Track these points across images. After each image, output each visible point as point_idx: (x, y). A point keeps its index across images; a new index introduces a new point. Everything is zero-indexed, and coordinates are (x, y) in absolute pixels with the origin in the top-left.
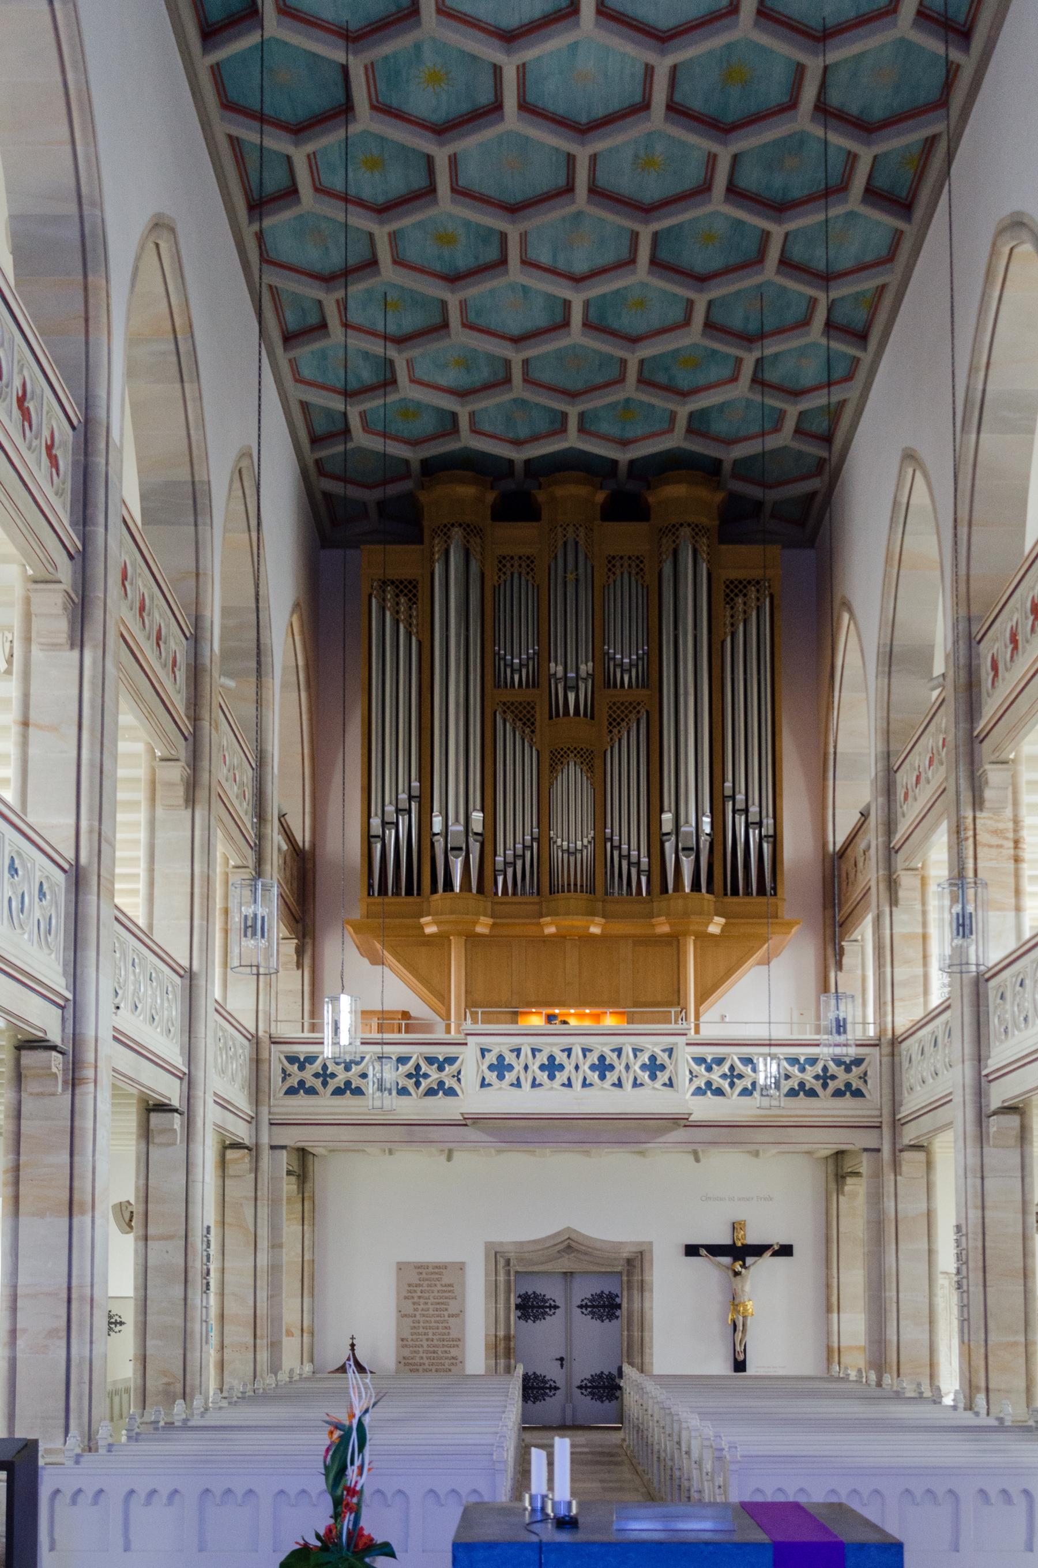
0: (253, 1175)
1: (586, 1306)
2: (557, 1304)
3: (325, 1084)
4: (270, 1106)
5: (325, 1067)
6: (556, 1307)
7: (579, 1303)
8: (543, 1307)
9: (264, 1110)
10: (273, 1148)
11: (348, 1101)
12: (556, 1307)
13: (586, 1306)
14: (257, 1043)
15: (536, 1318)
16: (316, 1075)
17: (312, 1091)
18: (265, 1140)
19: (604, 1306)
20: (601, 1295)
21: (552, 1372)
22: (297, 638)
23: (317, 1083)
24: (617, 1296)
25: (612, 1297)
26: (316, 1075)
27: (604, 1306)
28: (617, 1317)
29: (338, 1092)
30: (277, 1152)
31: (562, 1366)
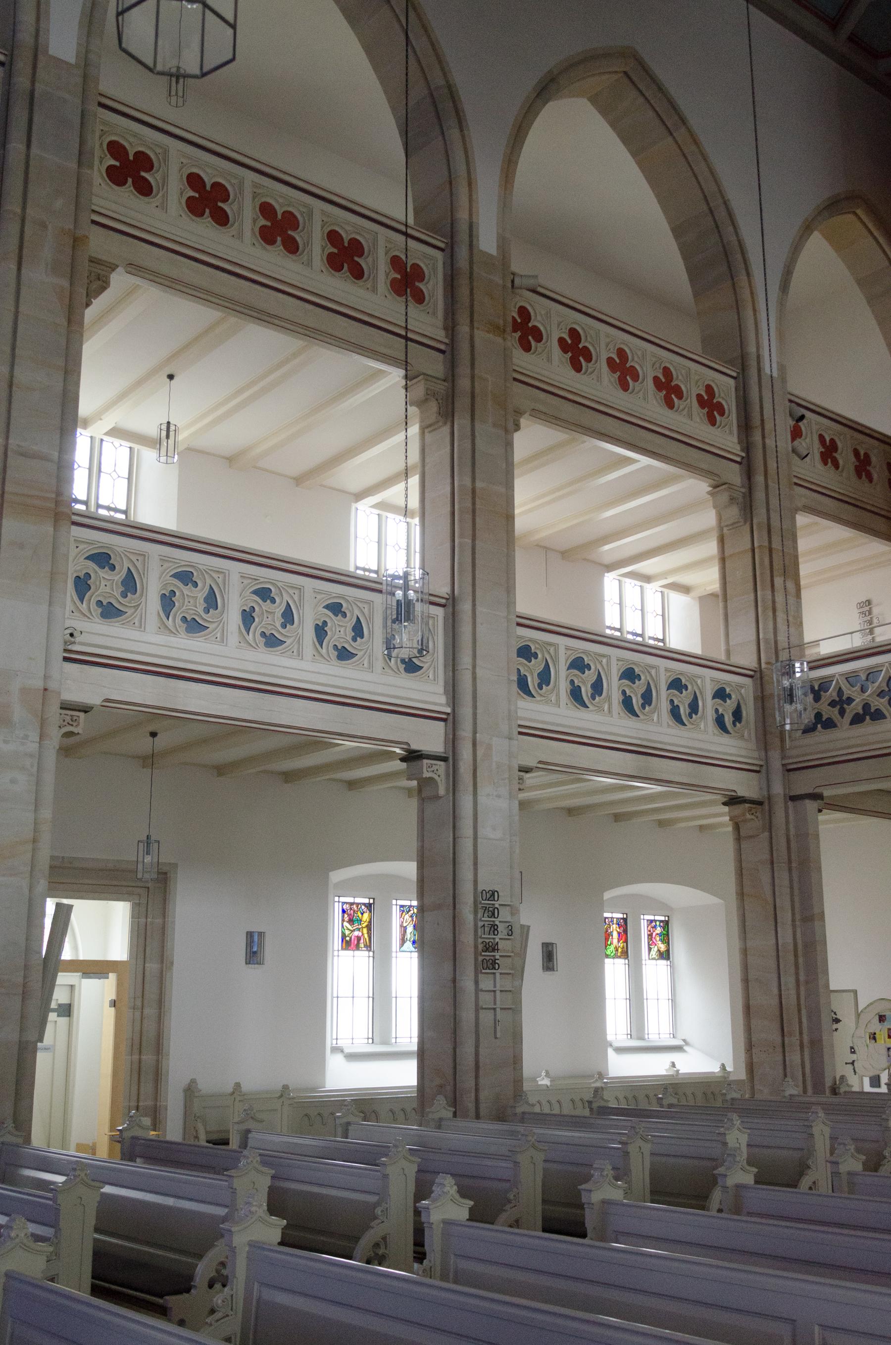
0: (767, 834)
3: (842, 712)
4: (783, 749)
5: (840, 692)
9: (775, 756)
10: (793, 798)
11: (869, 731)
14: (761, 678)
16: (833, 704)
17: (829, 724)
18: (778, 789)
22: (876, 233)
23: (834, 713)
26: (833, 704)
29: (857, 720)
30: (798, 803)
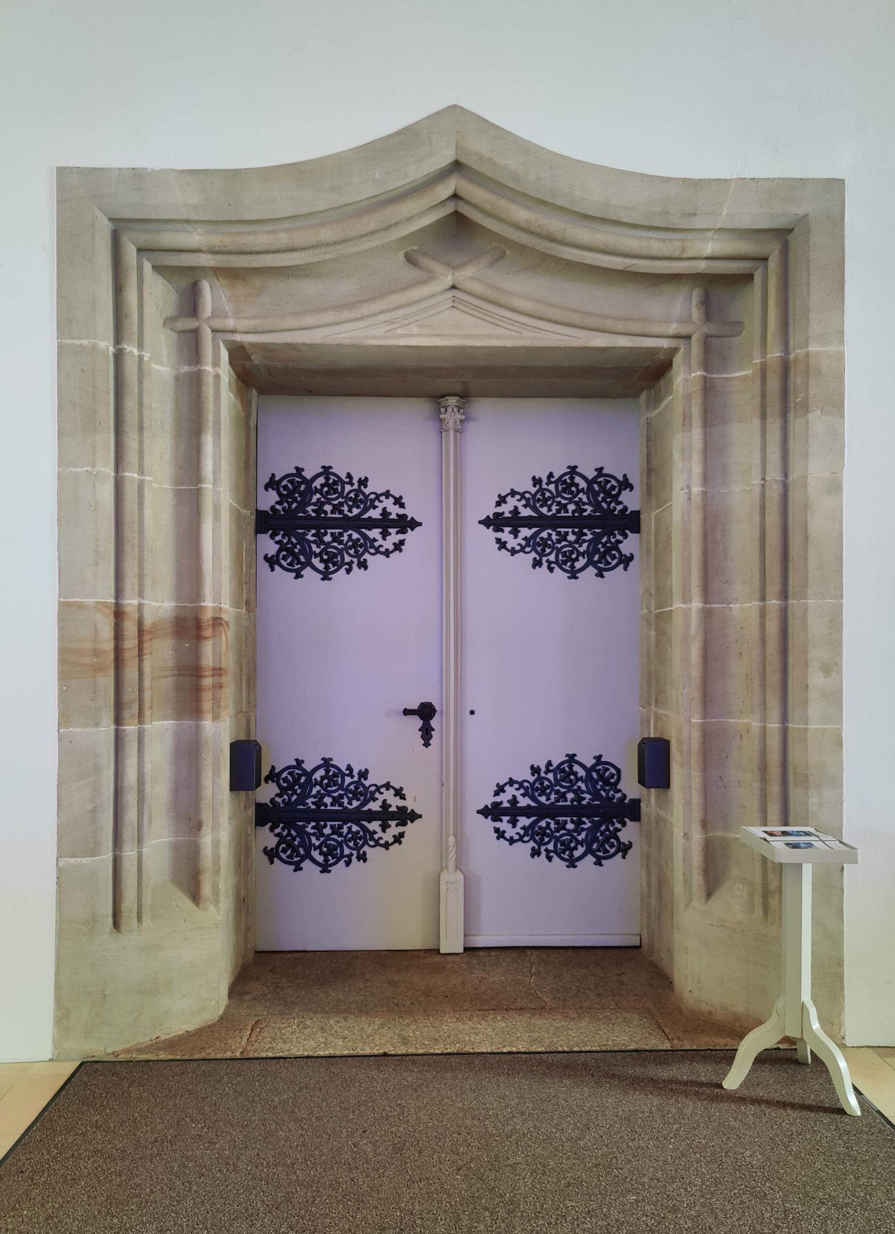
1: (515, 522)
2: (410, 512)
6: (406, 524)
7: (490, 510)
8: (360, 523)
12: (406, 524)
13: (515, 522)
15: (332, 564)
19: (578, 522)
20: (567, 482)
21: (379, 751)
24: (626, 484)
25: (606, 487)
27: (578, 522)
28: (626, 561)
31: (427, 733)
